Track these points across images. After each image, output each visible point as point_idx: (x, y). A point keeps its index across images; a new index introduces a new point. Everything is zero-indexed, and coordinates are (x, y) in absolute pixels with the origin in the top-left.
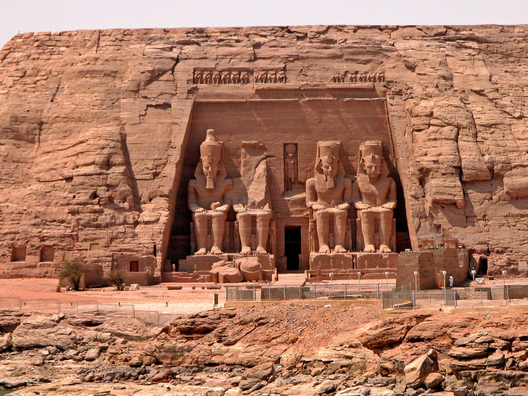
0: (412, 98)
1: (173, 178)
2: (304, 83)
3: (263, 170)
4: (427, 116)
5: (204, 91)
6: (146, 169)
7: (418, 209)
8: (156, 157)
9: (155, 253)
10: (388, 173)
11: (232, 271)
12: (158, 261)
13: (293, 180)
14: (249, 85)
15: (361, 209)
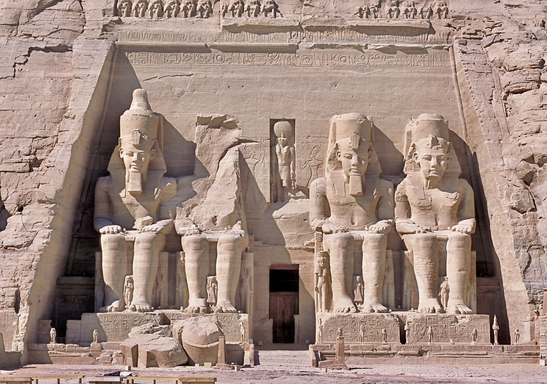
0: (501, 40)
1: (65, 170)
2: (308, 17)
3: (232, 164)
4: (533, 67)
5: (132, 27)
6: (17, 153)
7: (524, 233)
8: (36, 133)
9: (16, 307)
10: (459, 171)
11: (166, 344)
12: (21, 321)
13: (285, 184)
14: (213, 19)
15: (414, 233)
